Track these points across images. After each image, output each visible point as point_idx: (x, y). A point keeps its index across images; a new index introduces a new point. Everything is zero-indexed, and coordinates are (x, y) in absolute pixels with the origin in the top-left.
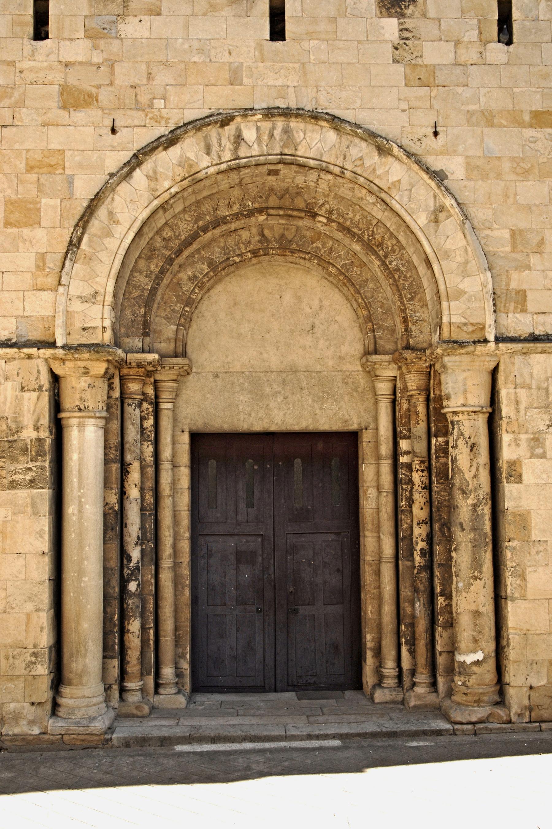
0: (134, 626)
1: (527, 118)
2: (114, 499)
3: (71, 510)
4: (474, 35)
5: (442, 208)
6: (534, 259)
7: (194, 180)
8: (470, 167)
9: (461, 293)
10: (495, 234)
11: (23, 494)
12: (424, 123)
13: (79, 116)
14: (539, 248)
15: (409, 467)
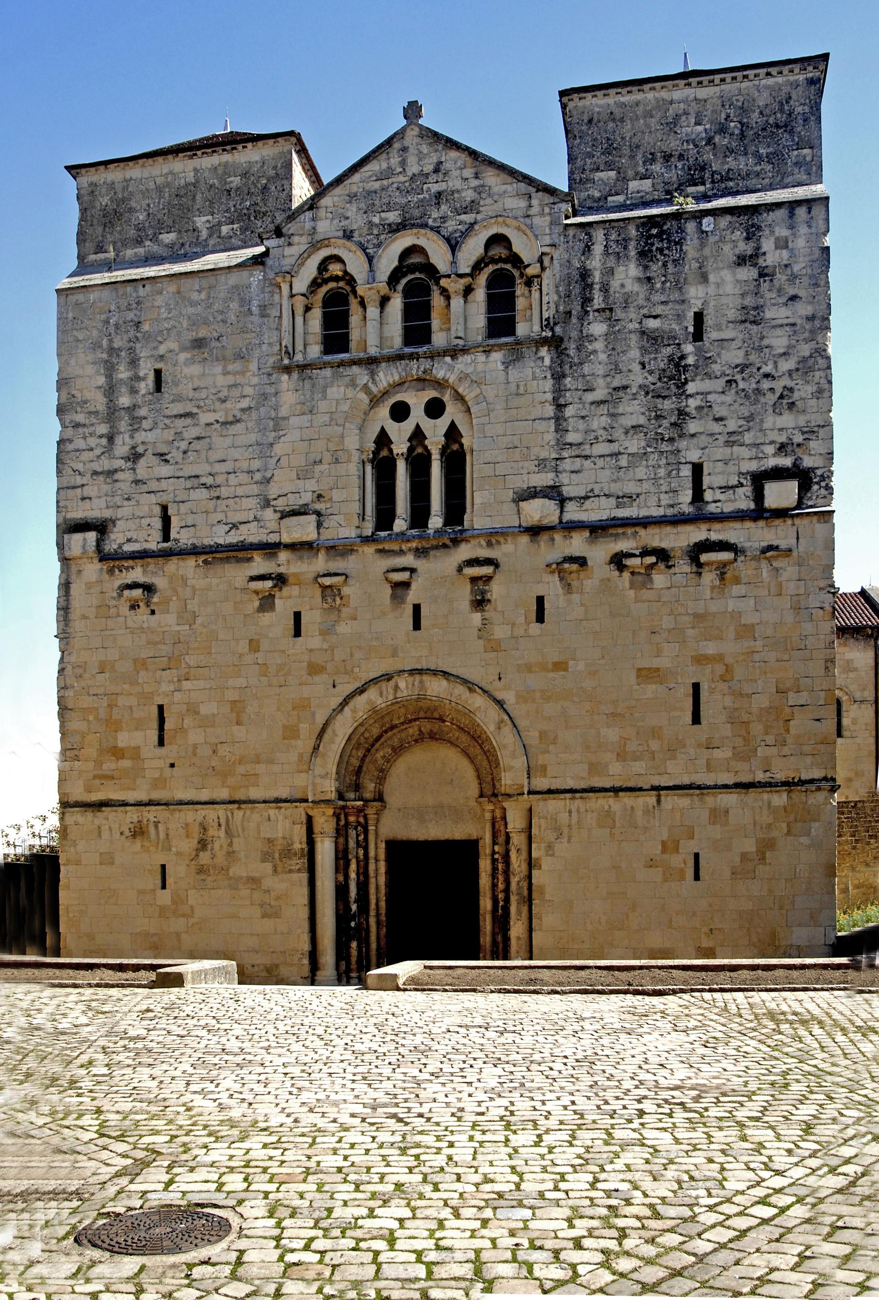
1: (550, 666)
5: (502, 721)
8: (518, 697)
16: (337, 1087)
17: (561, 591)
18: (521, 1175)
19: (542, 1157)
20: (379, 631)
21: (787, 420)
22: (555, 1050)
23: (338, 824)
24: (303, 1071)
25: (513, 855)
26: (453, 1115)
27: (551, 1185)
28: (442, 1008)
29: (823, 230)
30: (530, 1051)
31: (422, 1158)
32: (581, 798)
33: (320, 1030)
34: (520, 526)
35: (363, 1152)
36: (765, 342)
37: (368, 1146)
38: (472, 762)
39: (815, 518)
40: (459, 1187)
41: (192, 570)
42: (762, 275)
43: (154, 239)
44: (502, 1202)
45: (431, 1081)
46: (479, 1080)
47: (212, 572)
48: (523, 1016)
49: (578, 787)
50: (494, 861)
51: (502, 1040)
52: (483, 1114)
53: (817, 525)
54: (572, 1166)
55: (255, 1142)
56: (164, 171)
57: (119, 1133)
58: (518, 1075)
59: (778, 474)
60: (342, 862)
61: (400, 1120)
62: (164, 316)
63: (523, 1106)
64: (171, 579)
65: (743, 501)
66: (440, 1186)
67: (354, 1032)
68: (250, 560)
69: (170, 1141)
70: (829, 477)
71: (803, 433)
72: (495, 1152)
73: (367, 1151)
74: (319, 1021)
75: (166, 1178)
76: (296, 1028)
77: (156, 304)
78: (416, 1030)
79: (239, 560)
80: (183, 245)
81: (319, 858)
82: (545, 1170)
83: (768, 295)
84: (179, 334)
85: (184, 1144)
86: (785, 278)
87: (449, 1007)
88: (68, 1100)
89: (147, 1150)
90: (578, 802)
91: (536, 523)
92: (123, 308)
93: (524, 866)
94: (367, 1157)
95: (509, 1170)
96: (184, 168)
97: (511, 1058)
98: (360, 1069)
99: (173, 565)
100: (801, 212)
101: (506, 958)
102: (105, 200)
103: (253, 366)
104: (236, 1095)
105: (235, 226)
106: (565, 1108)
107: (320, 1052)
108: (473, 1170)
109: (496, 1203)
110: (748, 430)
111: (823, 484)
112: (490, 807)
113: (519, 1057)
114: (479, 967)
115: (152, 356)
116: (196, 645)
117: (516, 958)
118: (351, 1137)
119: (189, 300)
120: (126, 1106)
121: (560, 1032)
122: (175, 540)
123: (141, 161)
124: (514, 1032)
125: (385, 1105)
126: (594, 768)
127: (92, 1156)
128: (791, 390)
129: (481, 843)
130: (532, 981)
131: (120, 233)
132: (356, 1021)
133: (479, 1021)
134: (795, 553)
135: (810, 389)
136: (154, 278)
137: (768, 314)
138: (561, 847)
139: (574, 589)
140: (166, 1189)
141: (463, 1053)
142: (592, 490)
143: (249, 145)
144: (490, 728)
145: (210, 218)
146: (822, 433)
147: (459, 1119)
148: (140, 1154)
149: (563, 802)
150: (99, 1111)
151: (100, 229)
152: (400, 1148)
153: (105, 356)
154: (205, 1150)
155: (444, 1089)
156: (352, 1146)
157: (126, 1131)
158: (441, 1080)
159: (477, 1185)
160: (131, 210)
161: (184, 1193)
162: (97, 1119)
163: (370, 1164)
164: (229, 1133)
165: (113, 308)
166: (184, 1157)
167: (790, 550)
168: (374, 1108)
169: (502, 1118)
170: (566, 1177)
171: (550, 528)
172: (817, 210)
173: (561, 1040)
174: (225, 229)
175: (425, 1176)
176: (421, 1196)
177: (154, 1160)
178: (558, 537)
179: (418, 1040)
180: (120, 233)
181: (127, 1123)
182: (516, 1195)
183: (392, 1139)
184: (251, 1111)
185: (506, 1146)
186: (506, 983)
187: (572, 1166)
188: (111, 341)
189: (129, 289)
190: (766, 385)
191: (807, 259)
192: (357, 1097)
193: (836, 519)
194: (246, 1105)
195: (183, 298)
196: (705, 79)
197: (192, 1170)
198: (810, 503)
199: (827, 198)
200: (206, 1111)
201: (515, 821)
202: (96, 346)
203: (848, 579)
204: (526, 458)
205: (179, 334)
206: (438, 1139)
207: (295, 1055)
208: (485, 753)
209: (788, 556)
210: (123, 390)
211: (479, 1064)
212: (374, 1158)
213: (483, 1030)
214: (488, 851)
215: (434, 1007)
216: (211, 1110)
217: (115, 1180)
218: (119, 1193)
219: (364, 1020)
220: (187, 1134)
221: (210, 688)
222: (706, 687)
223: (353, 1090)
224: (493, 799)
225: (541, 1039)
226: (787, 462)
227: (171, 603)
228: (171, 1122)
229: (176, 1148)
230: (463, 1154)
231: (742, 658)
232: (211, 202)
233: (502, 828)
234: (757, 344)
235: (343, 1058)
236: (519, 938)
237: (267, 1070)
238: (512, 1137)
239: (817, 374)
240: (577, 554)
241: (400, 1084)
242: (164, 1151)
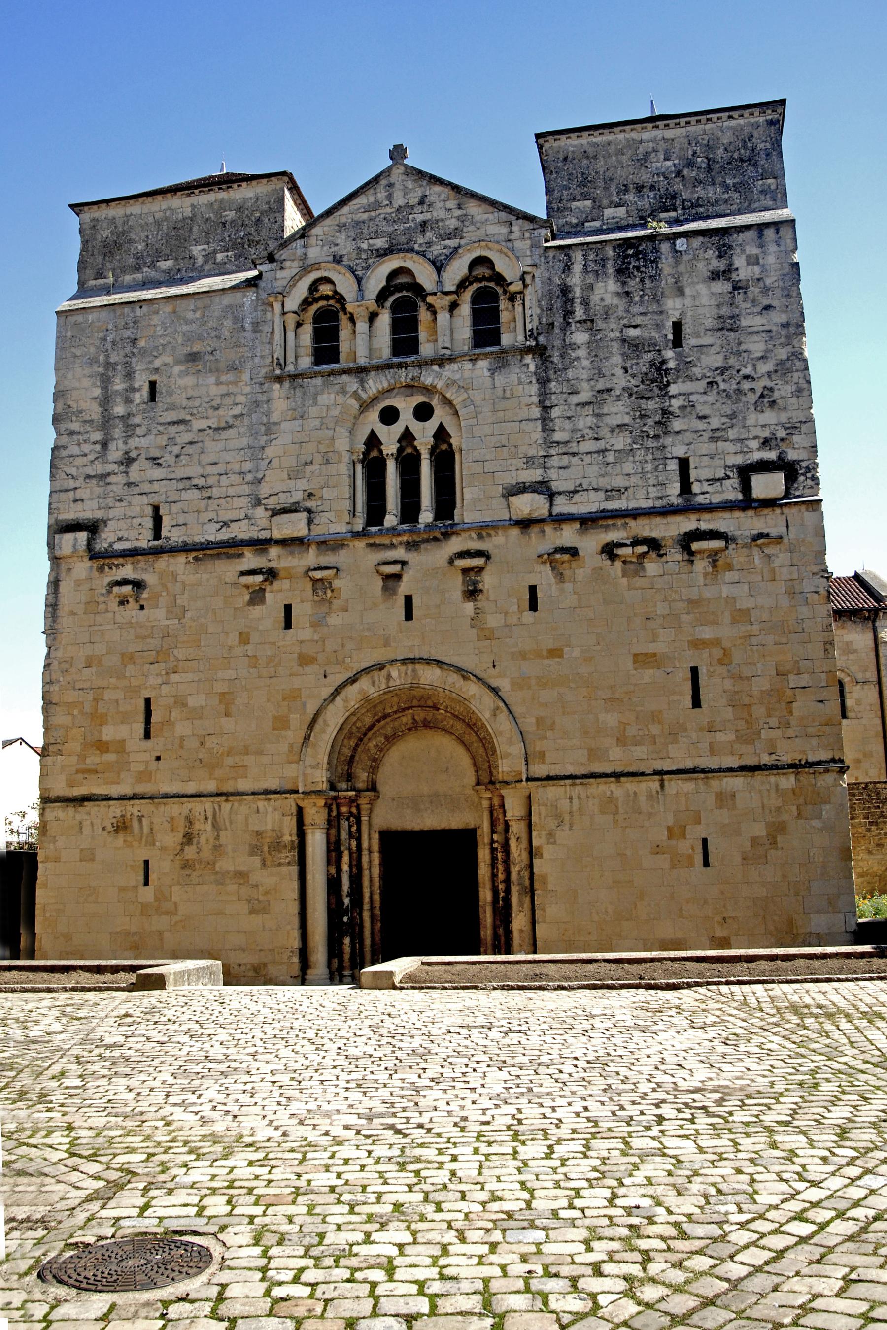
1: (545, 653)
4: (515, 608)
5: (498, 708)
6: (549, 734)
7: (366, 700)
8: (513, 684)
9: (508, 755)
10: (528, 720)
12: (487, 660)
13: (308, 669)
14: (552, 728)
16: (330, 1096)
17: (553, 580)
18: (531, 1192)
19: (555, 1170)
20: (368, 621)
21: (769, 417)
22: (564, 1051)
23: (329, 815)
24: (292, 1079)
25: (513, 843)
26: (456, 1125)
27: (564, 1203)
28: (442, 1007)
29: (791, 248)
30: (537, 1053)
31: (423, 1173)
32: (582, 784)
33: (311, 1034)
34: (510, 519)
35: (358, 1168)
36: (743, 347)
37: (364, 1162)
38: (468, 749)
39: (803, 507)
40: (464, 1206)
41: (182, 567)
42: (736, 288)
43: (152, 266)
44: (512, 1224)
45: (431, 1088)
46: (483, 1086)
47: (202, 568)
48: (529, 1014)
49: (578, 773)
50: (493, 850)
51: (507, 1041)
52: (487, 1123)
53: (806, 514)
54: (588, 1180)
55: (240, 1159)
56: (163, 208)
57: (91, 1152)
58: (525, 1079)
59: (764, 467)
60: (333, 854)
61: (398, 1132)
62: (160, 333)
63: (531, 1114)
64: (161, 575)
65: (731, 491)
66: (443, 1206)
67: (348, 1035)
68: (240, 556)
69: (147, 1160)
70: (814, 469)
71: (786, 428)
72: (503, 1166)
73: (363, 1167)
74: (310, 1024)
75: (141, 1202)
76: (285, 1032)
77: (152, 323)
78: (414, 1032)
79: (229, 556)
80: (179, 270)
81: (310, 850)
82: (557, 1185)
83: (743, 306)
84: (174, 349)
85: (162, 1163)
86: (757, 290)
87: (449, 1006)
88: (36, 1115)
89: (121, 1170)
90: (578, 788)
91: (526, 516)
92: (120, 327)
93: (525, 855)
94: (362, 1174)
95: (518, 1186)
96: (182, 205)
97: (516, 1060)
98: (354, 1076)
99: (163, 562)
100: (770, 233)
101: (508, 952)
102: (106, 233)
103: (246, 377)
104: (219, 1107)
105: (230, 254)
106: (577, 1114)
107: (311, 1057)
108: (479, 1187)
109: (505, 1224)
110: (732, 427)
111: (809, 475)
112: (488, 795)
113: (526, 1059)
114: (480, 963)
115: (147, 369)
116: (185, 639)
117: (519, 952)
118: (345, 1151)
119: (185, 319)
120: (99, 1121)
121: (569, 1031)
122: (166, 538)
123: (141, 200)
124: (520, 1032)
125: (381, 1115)
126: (593, 754)
127: (61, 1178)
128: (771, 390)
129: (479, 832)
130: (537, 977)
131: (119, 261)
132: (350, 1022)
133: (481, 1020)
134: (786, 540)
135: (789, 388)
136: (151, 300)
137: (744, 322)
138: (563, 835)
139: (566, 578)
140: (141, 1215)
141: (465, 1056)
142: (581, 485)
143: (244, 184)
144: (485, 716)
145: (206, 247)
146: (804, 428)
147: (463, 1129)
148: (113, 1175)
149: (563, 789)
150: (70, 1128)
151: (100, 259)
152: (398, 1163)
153: (101, 370)
154: (185, 1170)
155: (445, 1096)
156: (346, 1162)
157: (98, 1149)
158: (442, 1086)
159: (483, 1204)
160: (130, 241)
161: (161, 1219)
162: (67, 1136)
163: (366, 1182)
164: (212, 1149)
165: (110, 327)
166: (162, 1178)
167: (781, 538)
168: (370, 1119)
169: (509, 1128)
170: (582, 1193)
171: (541, 521)
172: (785, 231)
173: (571, 1040)
174: (220, 257)
175: (426, 1194)
176: (423, 1218)
177: (129, 1182)
178: (548, 529)
179: (416, 1043)
180: (119, 261)
181: (100, 1140)
182: (527, 1215)
183: (390, 1153)
184: (236, 1124)
185: (515, 1158)
186: (509, 979)
187: (588, 1180)
188: (107, 356)
189: (127, 310)
190: (746, 385)
191: (778, 273)
192: (351, 1106)
193: (824, 507)
194: (230, 1118)
195: (179, 318)
196: (672, 122)
197: (170, 1192)
198: (797, 493)
199: (793, 221)
200: (187, 1125)
201: (514, 809)
202: (93, 361)
203: (840, 563)
204: (514, 456)
205: (174, 349)
206: (440, 1152)
207: (284, 1061)
208: (481, 740)
209: (779, 543)
210: (118, 400)
211: (483, 1067)
212: (370, 1175)
213: (486, 1030)
214: (487, 840)
215: (432, 1007)
216: (192, 1124)
217: (86, 1206)
218: (89, 1220)
219: (358, 1021)
220: (165, 1152)
221: (199, 681)
222: (705, 671)
223: (346, 1099)
224: (490, 787)
225: (548, 1039)
226: (772, 455)
227: (161, 599)
228: (148, 1138)
229: (153, 1167)
230: (467, 1168)
231: (739, 642)
232: (207, 233)
233: (501, 816)
234: (735, 349)
235: (335, 1064)
236: (521, 931)
237: (254, 1078)
238: (521, 1148)
239: (796, 375)
240: (569, 545)
241: (397, 1091)
242: (139, 1171)
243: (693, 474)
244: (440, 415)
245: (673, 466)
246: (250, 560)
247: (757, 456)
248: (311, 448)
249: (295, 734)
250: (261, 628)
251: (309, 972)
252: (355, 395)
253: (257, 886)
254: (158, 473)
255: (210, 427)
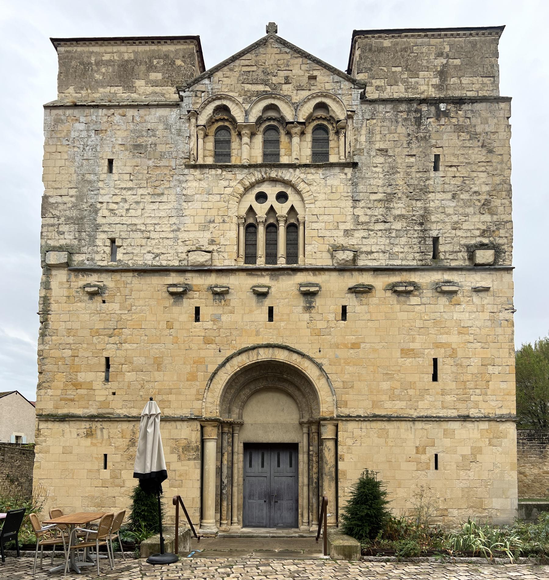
0: (225, 504)
2: (219, 464)
3: (206, 467)
11: (192, 463)
15: (312, 455)
243: (441, 248)
244: (293, 199)
245: (430, 242)
246: (173, 279)
247: (479, 239)
248: (214, 212)
249: (201, 383)
250: (180, 320)
251: (204, 521)
252: (241, 182)
253: (175, 471)
254: (117, 220)
255: (149, 194)
